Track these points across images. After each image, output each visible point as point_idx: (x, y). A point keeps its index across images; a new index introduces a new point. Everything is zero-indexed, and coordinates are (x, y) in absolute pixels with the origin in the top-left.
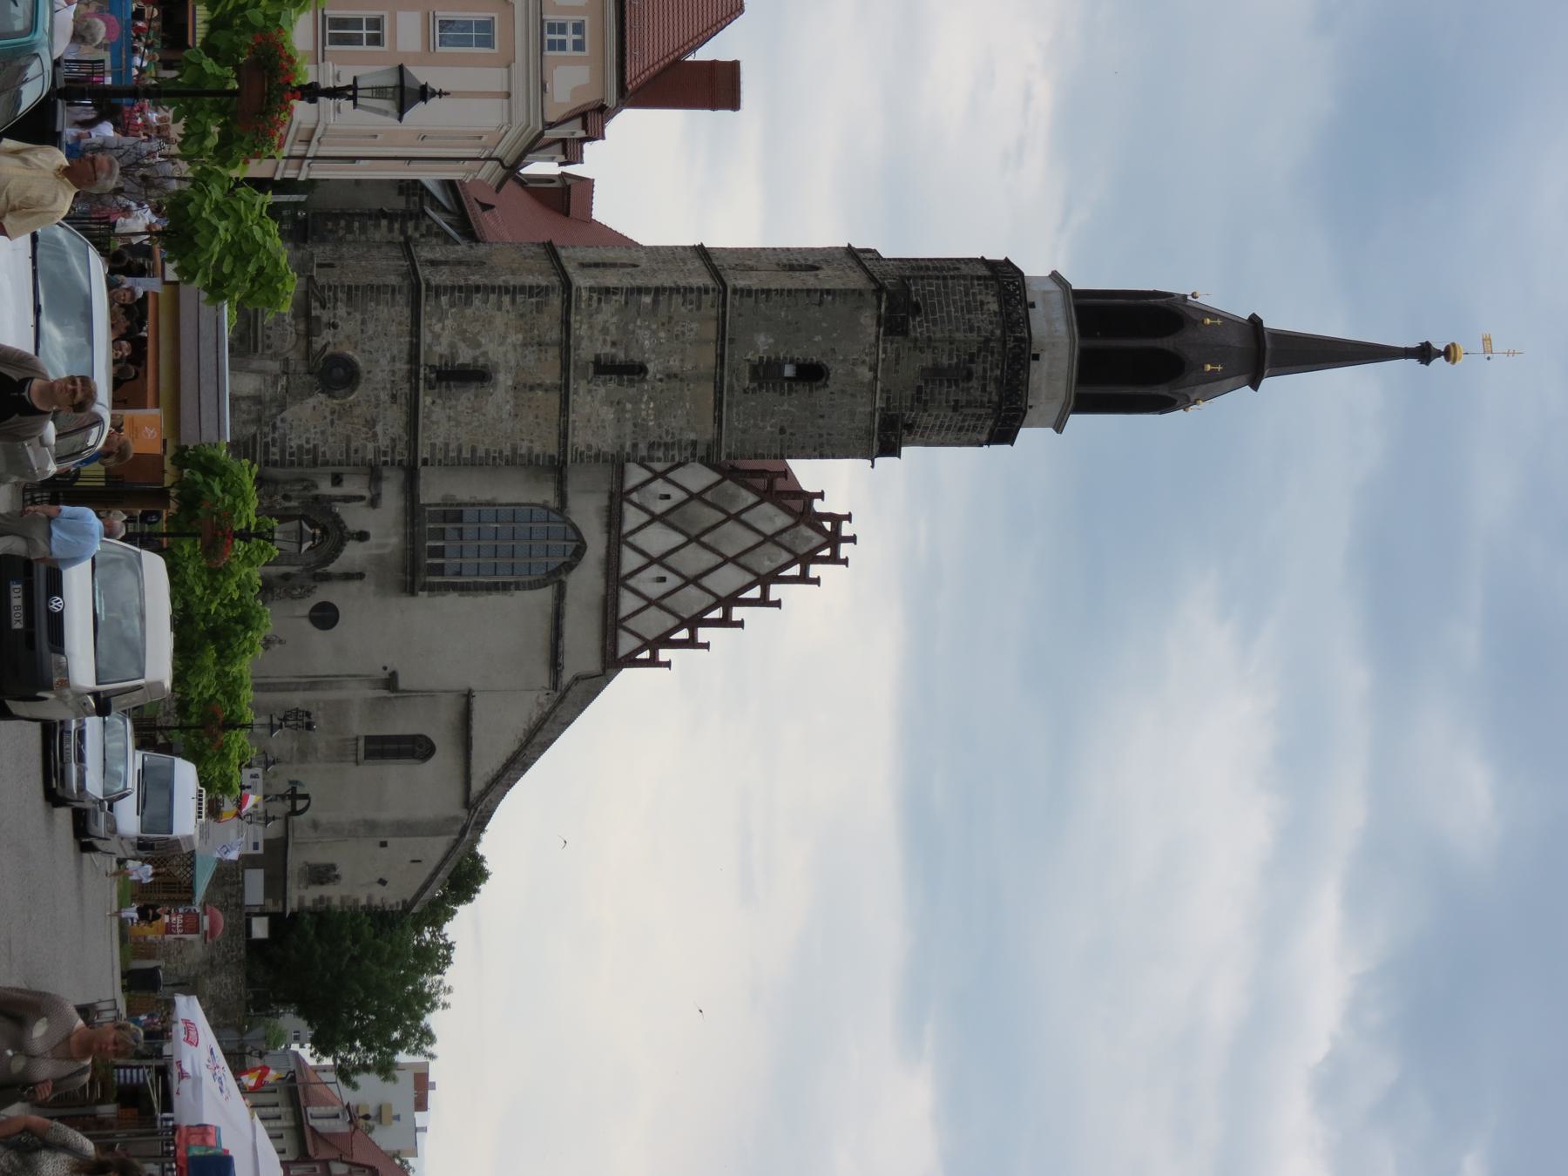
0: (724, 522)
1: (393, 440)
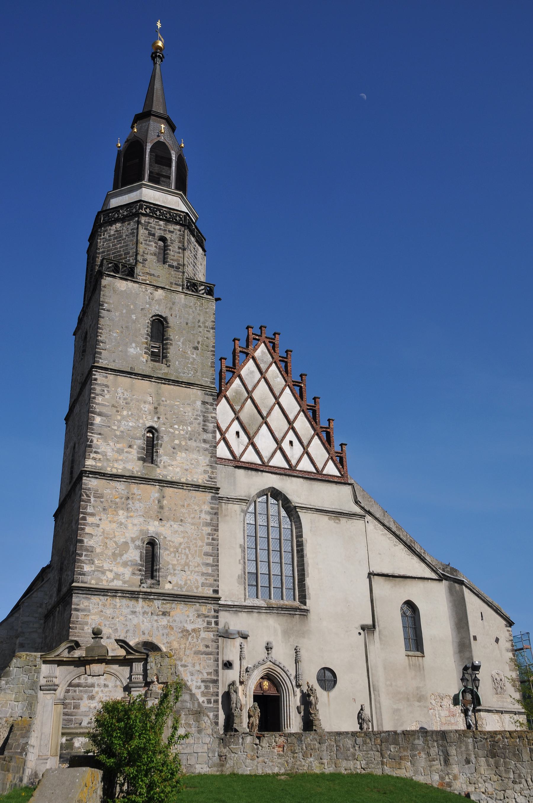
1: (199, 616)
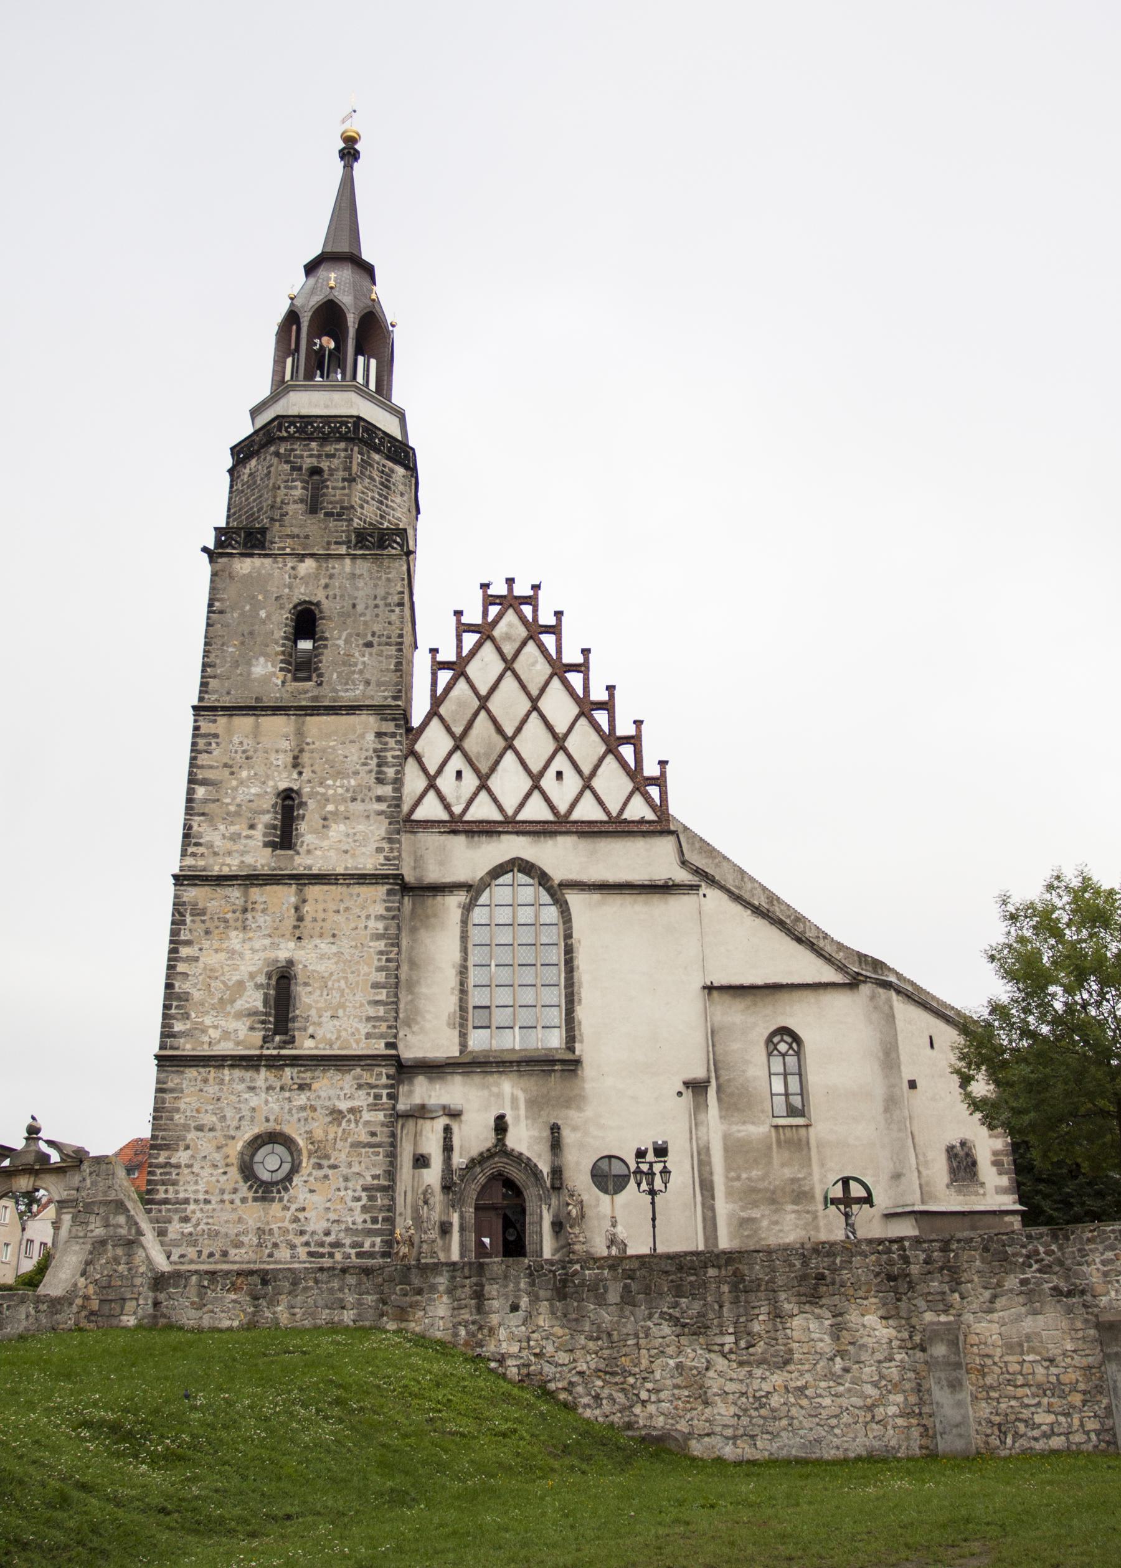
0: (489, 712)
1: (360, 1087)
